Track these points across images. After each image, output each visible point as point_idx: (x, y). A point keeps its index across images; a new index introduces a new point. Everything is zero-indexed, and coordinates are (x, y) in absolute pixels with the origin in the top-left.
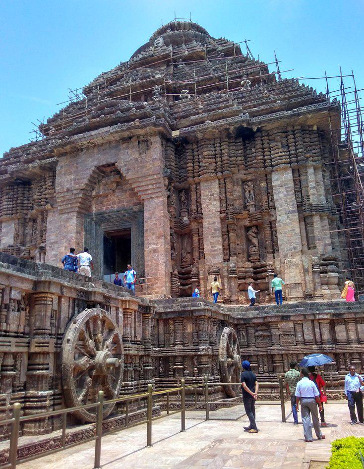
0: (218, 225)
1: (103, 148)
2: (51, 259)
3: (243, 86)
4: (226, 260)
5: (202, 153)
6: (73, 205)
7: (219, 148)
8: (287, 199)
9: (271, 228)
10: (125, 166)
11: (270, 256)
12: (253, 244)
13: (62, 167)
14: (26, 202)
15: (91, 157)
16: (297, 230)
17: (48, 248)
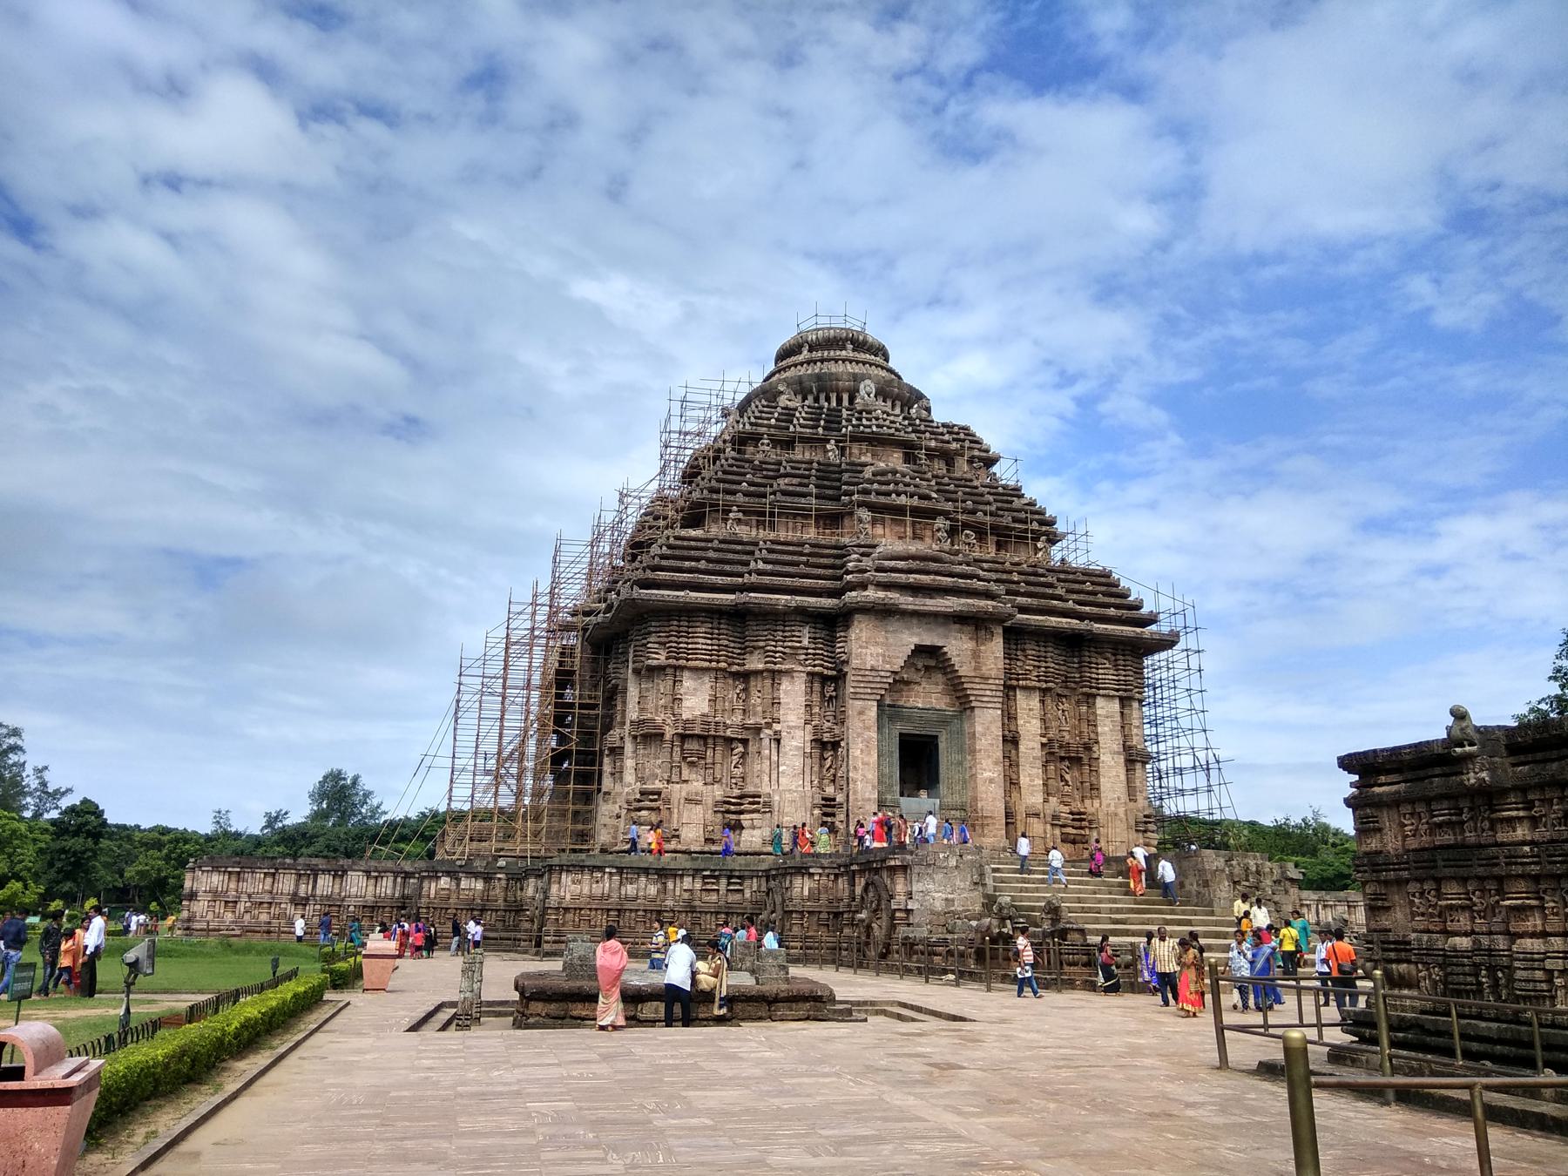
0: (1038, 752)
1: (925, 620)
2: (791, 753)
3: (1041, 550)
4: (1046, 801)
5: (1024, 650)
6: (875, 691)
7: (1042, 649)
8: (1113, 735)
9: (1090, 766)
10: (959, 655)
11: (1088, 802)
12: (1067, 781)
13: (861, 630)
14: (732, 645)
15: (908, 629)
16: (1123, 777)
17: (783, 734)
